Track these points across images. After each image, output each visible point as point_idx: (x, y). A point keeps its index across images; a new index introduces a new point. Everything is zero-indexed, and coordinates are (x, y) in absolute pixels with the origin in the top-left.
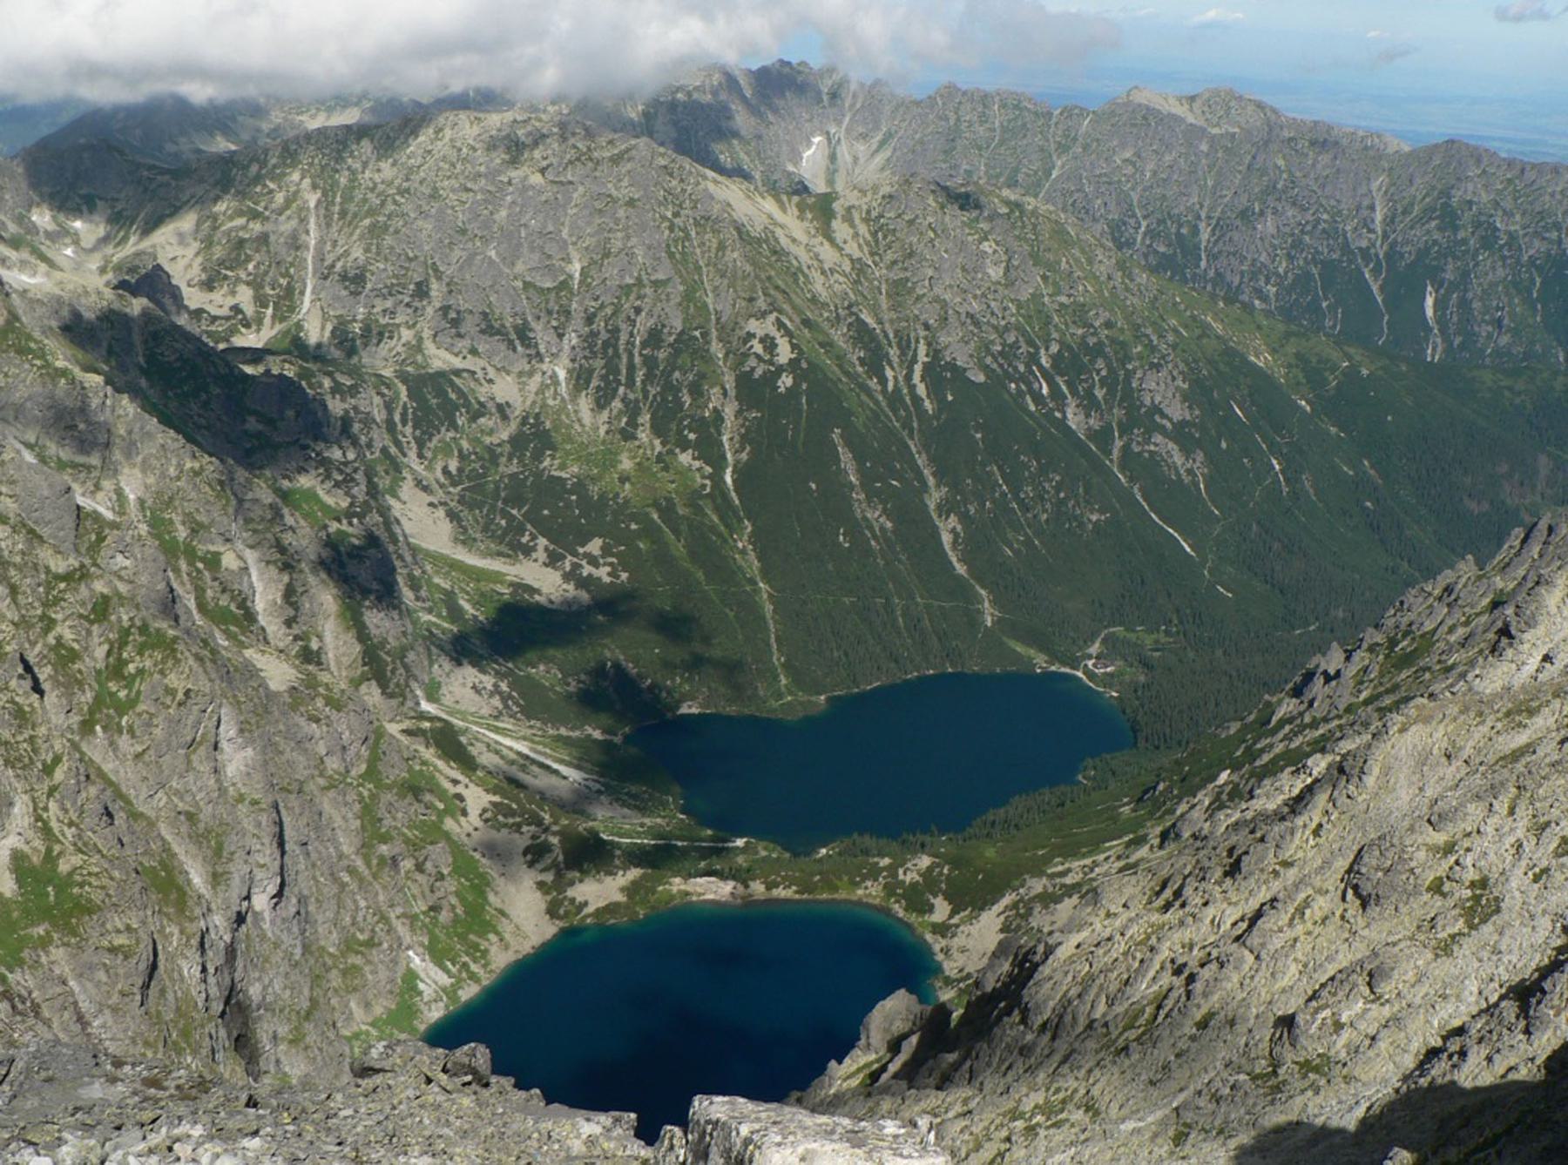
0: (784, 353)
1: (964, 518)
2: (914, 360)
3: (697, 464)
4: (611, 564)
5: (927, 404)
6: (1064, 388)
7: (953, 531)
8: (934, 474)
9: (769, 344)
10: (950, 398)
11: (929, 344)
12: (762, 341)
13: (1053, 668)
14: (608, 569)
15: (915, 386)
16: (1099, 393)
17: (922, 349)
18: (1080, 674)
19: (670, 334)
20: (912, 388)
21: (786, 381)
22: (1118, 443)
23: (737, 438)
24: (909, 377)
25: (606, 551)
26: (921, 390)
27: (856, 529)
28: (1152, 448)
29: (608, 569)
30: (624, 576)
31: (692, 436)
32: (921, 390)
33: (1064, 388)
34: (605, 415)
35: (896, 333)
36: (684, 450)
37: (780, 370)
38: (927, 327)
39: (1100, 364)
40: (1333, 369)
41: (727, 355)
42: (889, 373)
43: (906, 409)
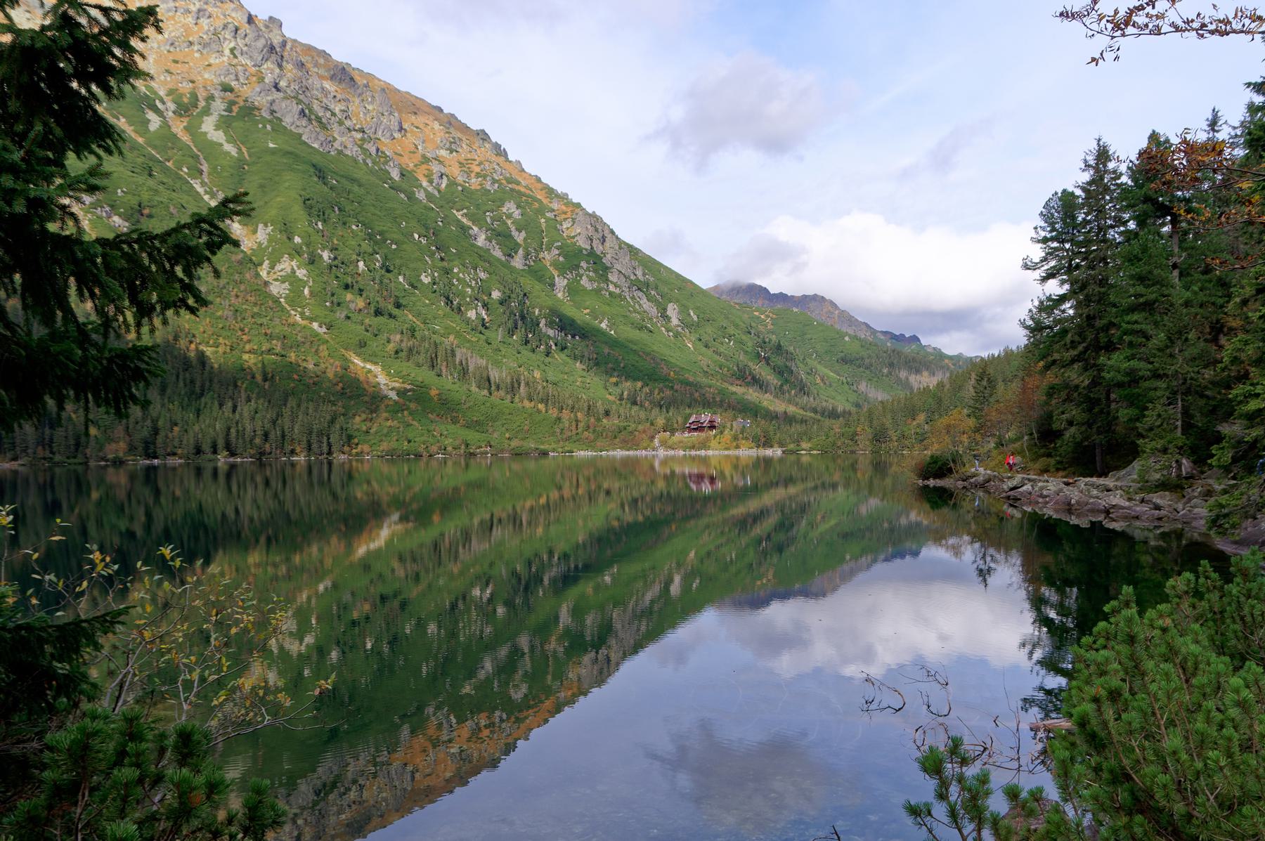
6: (465, 220)
28: (612, 288)
33: (465, 220)
39: (510, 207)
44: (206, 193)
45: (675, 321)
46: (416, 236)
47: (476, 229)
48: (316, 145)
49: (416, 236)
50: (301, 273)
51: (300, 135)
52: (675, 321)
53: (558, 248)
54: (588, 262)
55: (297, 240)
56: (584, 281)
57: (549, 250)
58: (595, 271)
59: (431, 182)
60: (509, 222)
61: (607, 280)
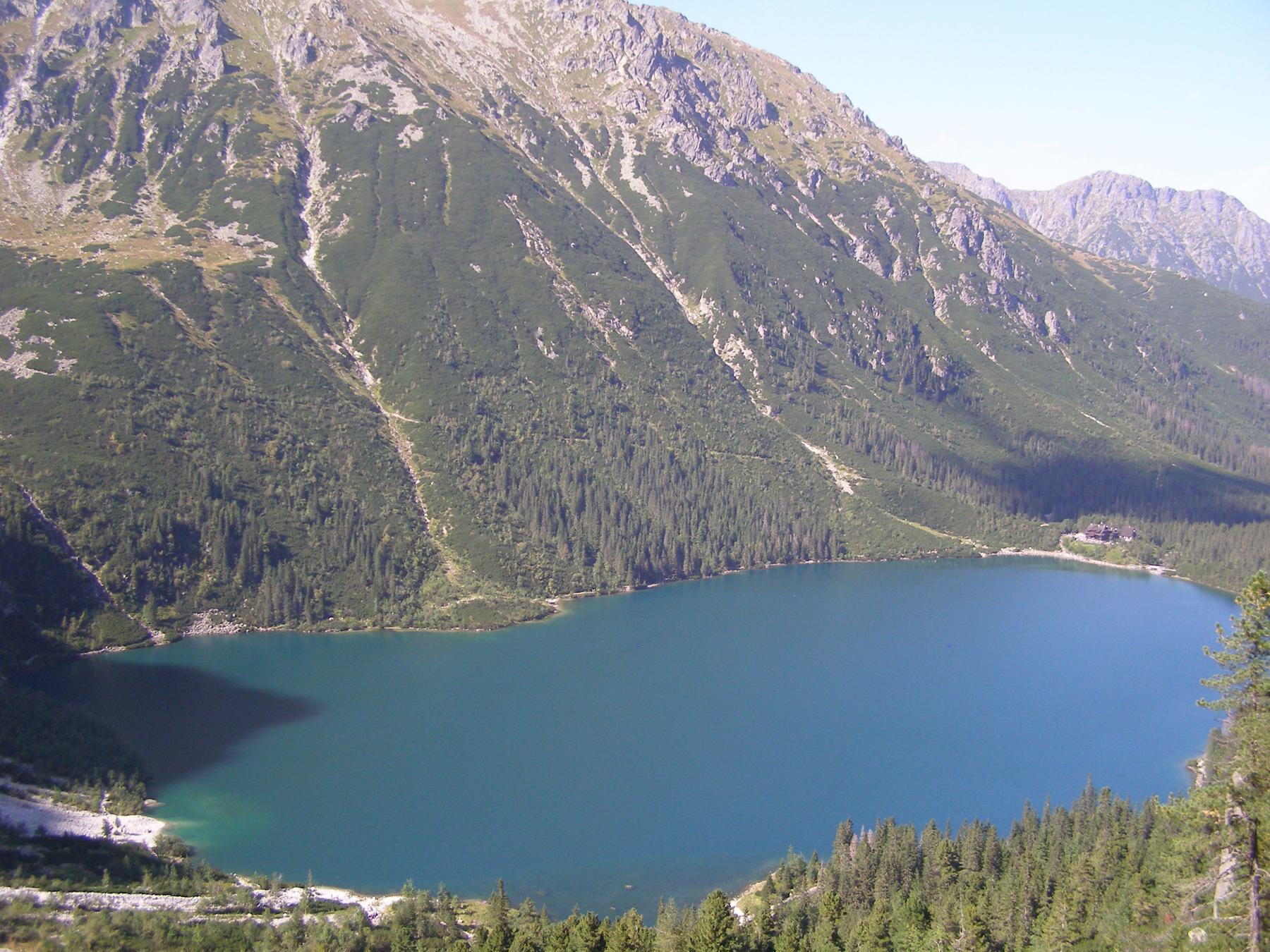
0: (406, 103)
1: (752, 342)
2: (619, 153)
3: (248, 239)
4: (41, 349)
5: (652, 201)
7: (740, 358)
8: (683, 290)
9: (383, 96)
10: (688, 194)
11: (639, 138)
12: (364, 89)
13: (1006, 551)
14: (30, 356)
15: (627, 183)
16: (894, 243)
17: (629, 144)
18: (1065, 555)
19: (203, 83)
20: (623, 186)
21: (413, 135)
22: (939, 296)
23: (324, 210)
24: (614, 173)
25: (27, 329)
26: (638, 185)
27: (570, 333)
29: (30, 356)
30: (65, 364)
31: (238, 205)
32: (638, 185)
33: (841, 227)
34: (76, 189)
35: (584, 127)
36: (222, 222)
37: (405, 120)
38: (631, 119)
39: (882, 203)
40: (1145, 277)
41: (305, 110)
42: (580, 166)
43: (618, 206)
44: (648, 260)
45: (1052, 331)
46: (818, 280)
47: (855, 239)
48: (718, 181)
49: (818, 280)
50: (747, 353)
51: (702, 169)
52: (1052, 331)
53: (935, 254)
54: (967, 274)
55: (736, 314)
56: (963, 296)
57: (925, 254)
58: (974, 285)
59: (805, 181)
60: (883, 222)
61: (987, 293)
